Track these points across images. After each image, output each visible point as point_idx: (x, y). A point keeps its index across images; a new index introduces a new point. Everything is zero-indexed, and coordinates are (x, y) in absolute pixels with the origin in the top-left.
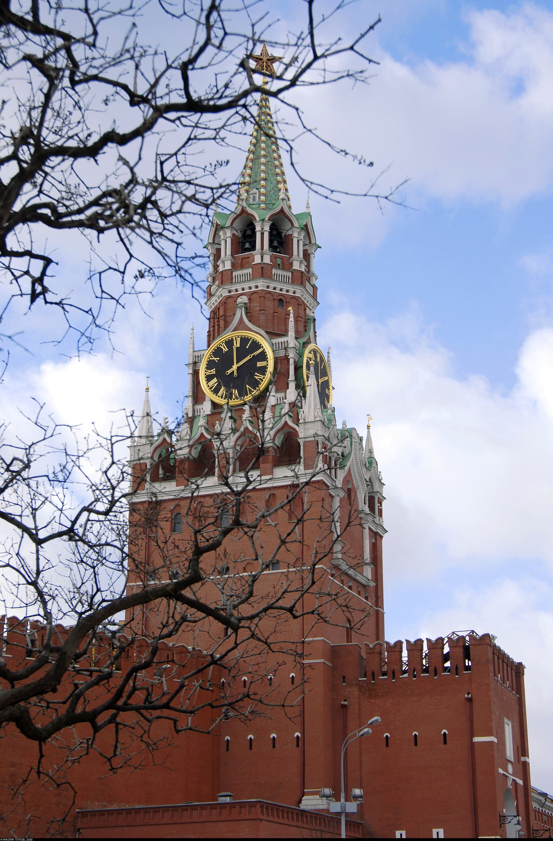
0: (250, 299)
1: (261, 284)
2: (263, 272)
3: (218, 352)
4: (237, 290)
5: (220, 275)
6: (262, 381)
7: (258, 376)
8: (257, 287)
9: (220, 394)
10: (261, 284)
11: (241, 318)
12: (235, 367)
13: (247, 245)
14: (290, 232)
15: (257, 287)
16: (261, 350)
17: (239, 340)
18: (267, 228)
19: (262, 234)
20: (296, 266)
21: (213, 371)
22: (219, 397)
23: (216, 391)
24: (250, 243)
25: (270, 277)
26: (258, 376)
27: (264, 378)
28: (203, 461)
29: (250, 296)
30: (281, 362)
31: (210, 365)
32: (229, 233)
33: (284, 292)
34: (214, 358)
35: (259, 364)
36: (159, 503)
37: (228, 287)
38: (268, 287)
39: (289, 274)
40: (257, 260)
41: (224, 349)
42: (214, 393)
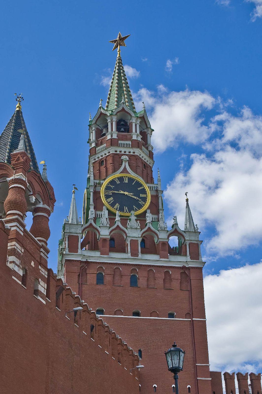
0: (129, 158)
1: (138, 152)
2: (136, 144)
4: (120, 152)
5: (110, 140)
6: (144, 206)
9: (115, 207)
10: (138, 152)
11: (125, 168)
12: (126, 193)
14: (146, 130)
16: (142, 188)
17: (127, 179)
18: (138, 122)
19: (136, 125)
20: (150, 149)
22: (115, 209)
23: (113, 205)
24: (124, 129)
25: (141, 149)
27: (145, 204)
28: (116, 244)
29: (130, 156)
32: (115, 119)
34: (111, 186)
35: (141, 195)
36: (87, 263)
38: (140, 155)
39: (148, 152)
40: (134, 137)
41: (117, 182)
42: (111, 206)
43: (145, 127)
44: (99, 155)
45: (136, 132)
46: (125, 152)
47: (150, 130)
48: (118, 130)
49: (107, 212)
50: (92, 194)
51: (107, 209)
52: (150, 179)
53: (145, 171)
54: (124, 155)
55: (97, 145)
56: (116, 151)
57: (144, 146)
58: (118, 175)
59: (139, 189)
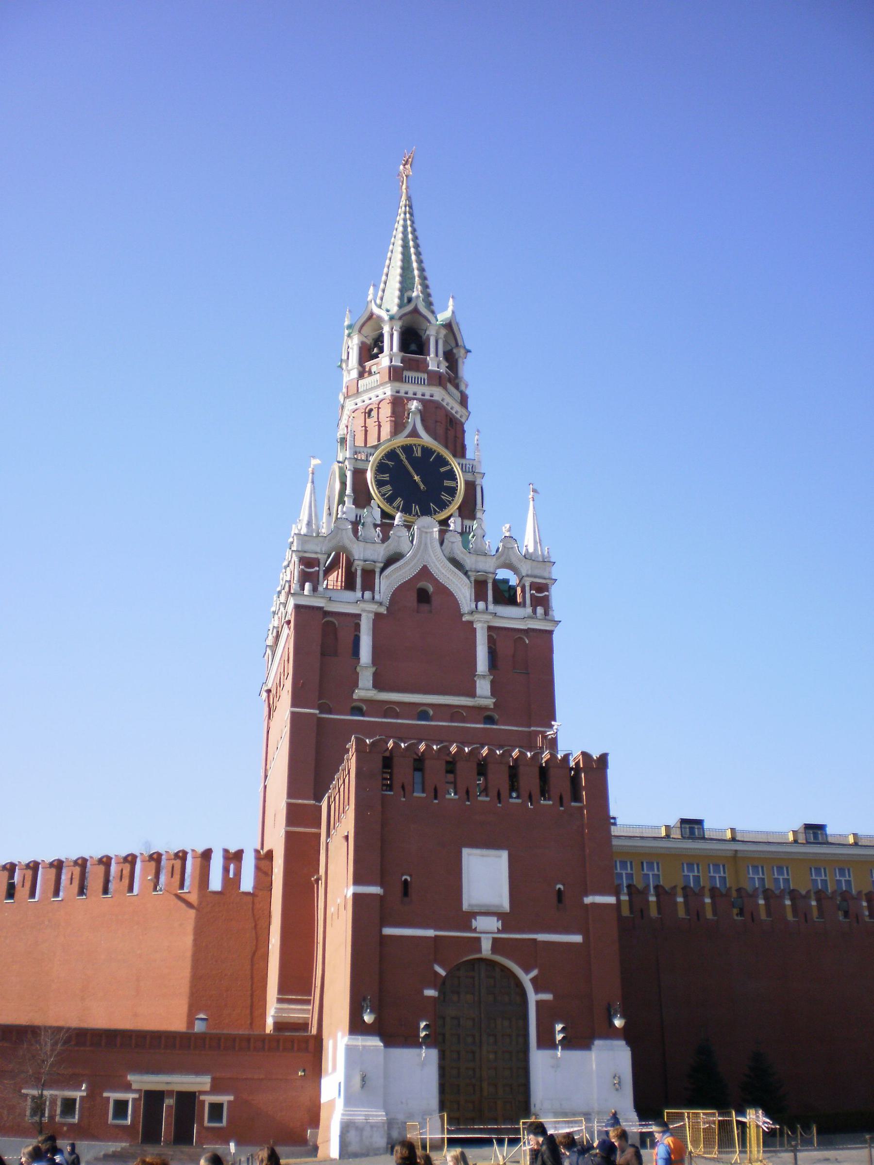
0: (424, 406)
1: (438, 394)
2: (437, 380)
3: (391, 455)
4: (406, 393)
7: (445, 497)
8: (432, 396)
9: (395, 504)
13: (413, 347)
15: (432, 396)
20: (462, 387)
21: (386, 477)
23: (390, 500)
25: (445, 388)
26: (445, 497)
30: (471, 486)
31: (381, 468)
33: (453, 412)
35: (447, 483)
37: (397, 385)
39: (459, 395)
43: (453, 345)
44: (365, 397)
45: (437, 355)
46: (415, 394)
47: (462, 351)
48: (404, 346)
49: (377, 514)
50: (349, 474)
51: (379, 507)
52: (460, 451)
53: (451, 433)
54: (414, 399)
55: (361, 375)
56: (398, 392)
57: (450, 382)
58: (402, 440)
59: (442, 470)
